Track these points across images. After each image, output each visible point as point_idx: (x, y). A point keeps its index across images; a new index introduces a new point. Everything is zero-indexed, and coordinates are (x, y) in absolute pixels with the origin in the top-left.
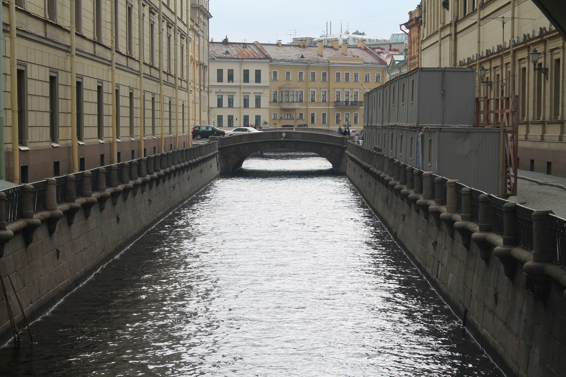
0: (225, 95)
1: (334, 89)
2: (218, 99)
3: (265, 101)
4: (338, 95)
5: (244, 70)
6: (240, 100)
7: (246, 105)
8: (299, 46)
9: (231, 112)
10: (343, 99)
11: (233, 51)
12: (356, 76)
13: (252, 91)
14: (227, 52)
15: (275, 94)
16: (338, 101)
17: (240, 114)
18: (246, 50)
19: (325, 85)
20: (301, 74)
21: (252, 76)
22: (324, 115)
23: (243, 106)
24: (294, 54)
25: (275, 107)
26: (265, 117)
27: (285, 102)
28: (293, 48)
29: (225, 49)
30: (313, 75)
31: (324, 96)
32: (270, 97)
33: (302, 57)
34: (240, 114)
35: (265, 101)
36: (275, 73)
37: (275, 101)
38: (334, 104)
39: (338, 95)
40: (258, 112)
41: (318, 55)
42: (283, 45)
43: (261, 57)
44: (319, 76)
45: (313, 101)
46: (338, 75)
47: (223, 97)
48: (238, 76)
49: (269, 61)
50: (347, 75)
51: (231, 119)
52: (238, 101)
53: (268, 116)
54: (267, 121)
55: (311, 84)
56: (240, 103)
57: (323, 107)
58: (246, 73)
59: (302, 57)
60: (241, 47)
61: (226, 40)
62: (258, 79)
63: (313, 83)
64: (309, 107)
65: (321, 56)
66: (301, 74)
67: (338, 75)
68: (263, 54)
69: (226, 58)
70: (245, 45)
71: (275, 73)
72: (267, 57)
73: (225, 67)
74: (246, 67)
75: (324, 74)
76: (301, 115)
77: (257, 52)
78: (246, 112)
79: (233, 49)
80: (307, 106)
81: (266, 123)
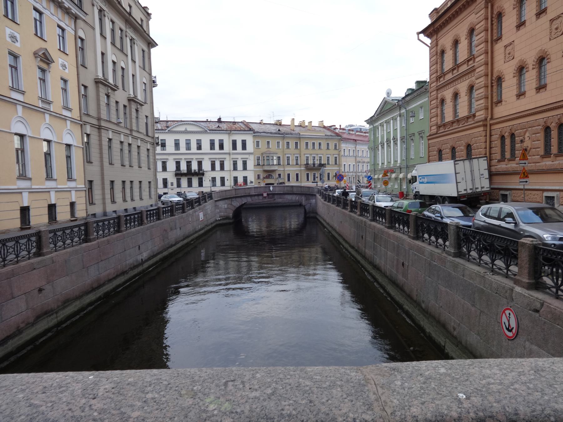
0: (217, 160)
1: (305, 154)
2: (211, 164)
3: (251, 165)
4: (307, 160)
5: (233, 140)
6: (230, 164)
7: (235, 168)
8: (277, 124)
9: (222, 174)
10: (311, 162)
11: (224, 126)
12: (320, 144)
13: (239, 157)
14: (218, 126)
15: (258, 159)
16: (307, 164)
17: (230, 176)
18: (235, 125)
19: (297, 151)
20: (278, 143)
21: (239, 145)
22: (297, 175)
23: (232, 169)
24: (274, 129)
25: (259, 169)
26: (251, 177)
27: (267, 165)
28: (272, 125)
29: (217, 125)
30: (288, 143)
31: (297, 160)
32: (254, 160)
33: (279, 130)
34: (230, 176)
35: (251, 165)
36: (258, 142)
37: (258, 165)
38: (305, 166)
39: (307, 160)
40: (245, 173)
41: (291, 130)
42: (264, 124)
43: (246, 129)
44: (292, 145)
45: (288, 164)
46: (307, 143)
47: (216, 162)
48: (228, 146)
49: (252, 132)
50: (314, 144)
51: (223, 179)
52: (228, 165)
53: (253, 176)
54: (253, 180)
55: (287, 151)
56: (230, 168)
57: (297, 168)
58: (234, 143)
59: (279, 130)
60: (231, 124)
61: (220, 119)
62: (244, 147)
63: (288, 150)
64: (286, 169)
65: (294, 131)
66: (278, 143)
67: (307, 143)
68: (248, 127)
69: (218, 130)
70: (234, 123)
71: (258, 142)
72: (251, 130)
73: (217, 138)
74: (234, 137)
75: (296, 143)
76: (280, 175)
77: (244, 126)
78: (235, 174)
79: (225, 125)
80: (284, 168)
81: (252, 182)
